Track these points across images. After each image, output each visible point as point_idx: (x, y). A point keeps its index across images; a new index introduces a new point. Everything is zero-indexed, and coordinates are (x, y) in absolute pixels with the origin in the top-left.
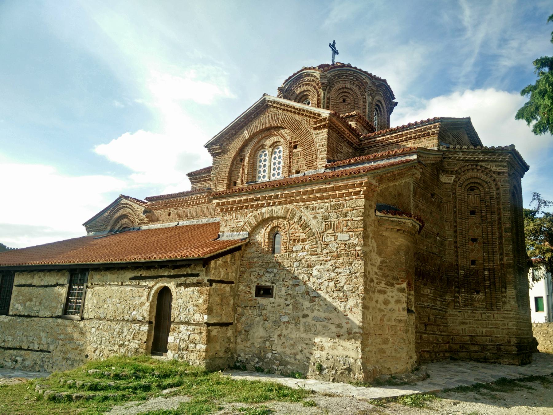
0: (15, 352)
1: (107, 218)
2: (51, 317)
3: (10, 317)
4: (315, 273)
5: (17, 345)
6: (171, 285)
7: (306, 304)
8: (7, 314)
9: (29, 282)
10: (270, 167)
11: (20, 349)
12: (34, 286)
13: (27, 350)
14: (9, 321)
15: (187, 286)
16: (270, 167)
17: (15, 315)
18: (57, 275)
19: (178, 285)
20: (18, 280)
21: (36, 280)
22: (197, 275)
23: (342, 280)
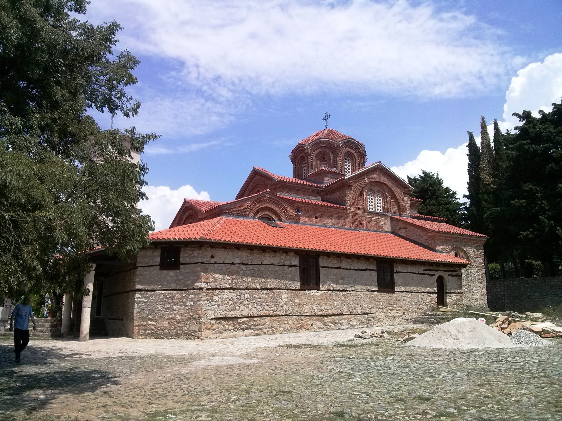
0: (337, 317)
1: (250, 206)
2: (367, 291)
3: (324, 292)
4: (473, 273)
5: (339, 312)
6: (445, 275)
7: (472, 285)
8: (318, 289)
9: (336, 266)
10: (375, 204)
11: (342, 314)
12: (343, 269)
13: (350, 314)
14: (322, 295)
15: (452, 276)
16: (375, 204)
17: (328, 290)
18: (365, 263)
19: (449, 275)
20: (323, 262)
21: (344, 265)
22: (456, 271)
23: (480, 276)
